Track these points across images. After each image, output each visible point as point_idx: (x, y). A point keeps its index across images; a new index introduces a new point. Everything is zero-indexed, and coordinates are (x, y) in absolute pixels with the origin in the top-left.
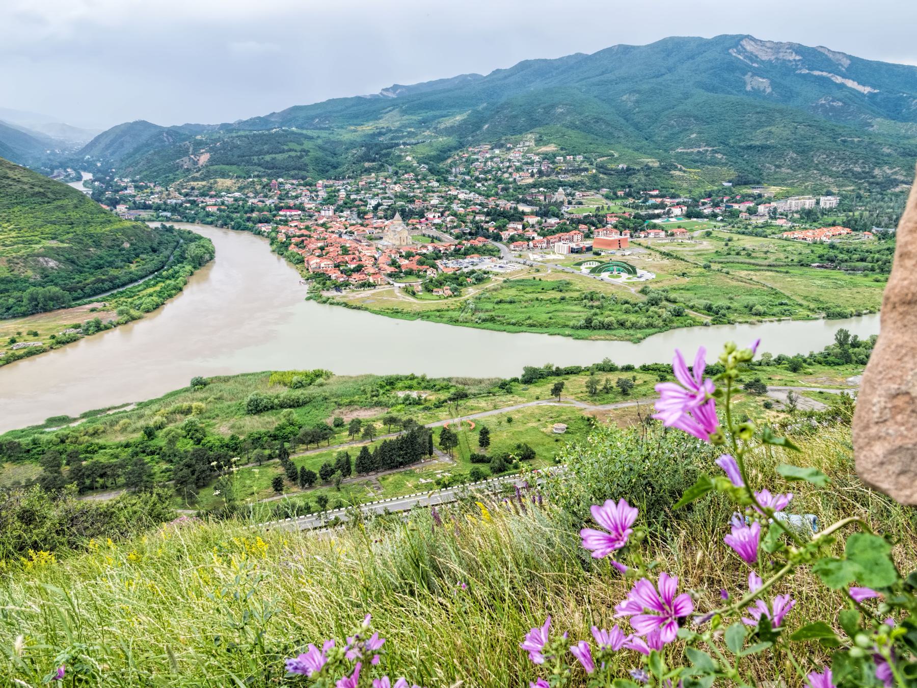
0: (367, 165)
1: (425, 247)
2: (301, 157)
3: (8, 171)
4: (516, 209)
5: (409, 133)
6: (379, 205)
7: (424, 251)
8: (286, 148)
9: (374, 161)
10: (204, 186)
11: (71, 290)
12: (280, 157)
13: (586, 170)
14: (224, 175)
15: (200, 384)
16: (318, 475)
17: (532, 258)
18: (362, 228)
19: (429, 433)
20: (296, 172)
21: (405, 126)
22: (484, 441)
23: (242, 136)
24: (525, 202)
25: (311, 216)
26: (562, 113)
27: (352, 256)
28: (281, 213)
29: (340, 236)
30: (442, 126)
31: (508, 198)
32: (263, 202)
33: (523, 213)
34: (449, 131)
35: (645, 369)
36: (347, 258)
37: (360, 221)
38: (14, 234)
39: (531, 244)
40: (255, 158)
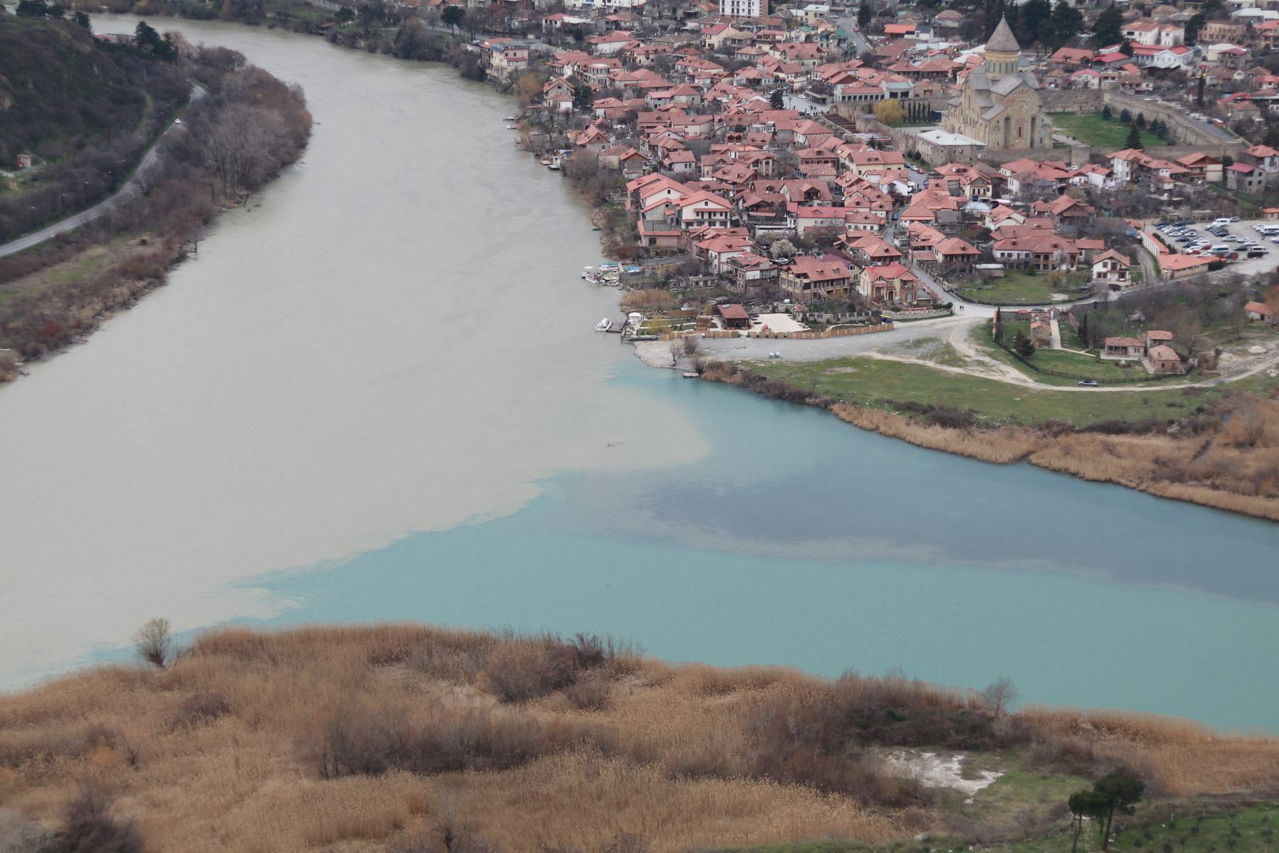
1: (1098, 160)
7: (1097, 179)
18: (865, 73)
27: (806, 187)
29: (776, 102)
37: (861, 44)
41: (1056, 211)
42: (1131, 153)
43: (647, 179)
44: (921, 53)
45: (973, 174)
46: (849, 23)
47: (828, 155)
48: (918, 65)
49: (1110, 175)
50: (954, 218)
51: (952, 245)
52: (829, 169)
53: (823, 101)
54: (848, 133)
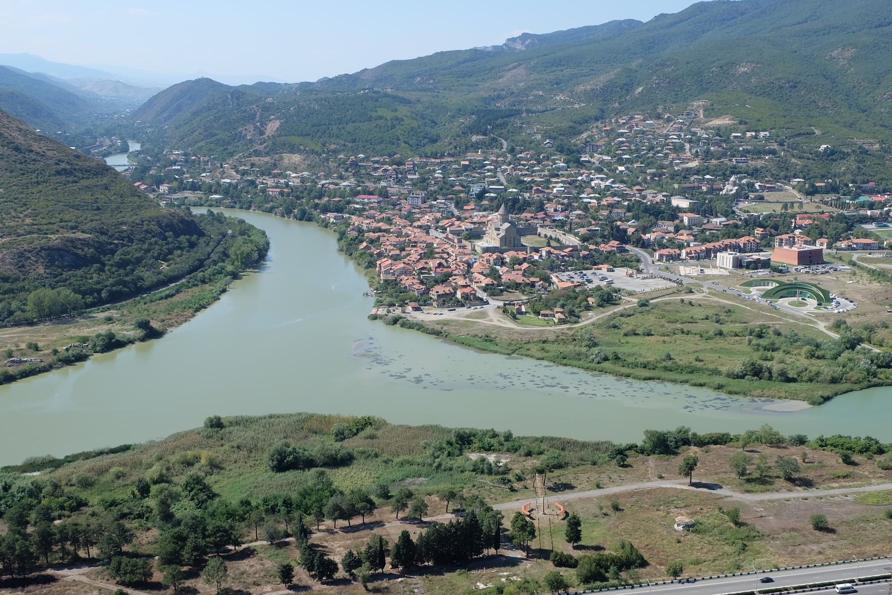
0: (474, 138)
1: (536, 250)
4: (670, 202)
5: (536, 96)
6: (484, 191)
7: (536, 257)
8: (374, 114)
9: (485, 134)
13: (773, 152)
14: (293, 150)
16: (340, 566)
17: (682, 273)
18: (457, 223)
19: (497, 518)
21: (532, 88)
22: (574, 532)
24: (682, 193)
25: (394, 205)
26: (745, 73)
27: (438, 261)
29: (428, 233)
31: (661, 187)
32: (337, 184)
33: (679, 209)
34: (590, 96)
35: (823, 444)
36: (432, 264)
37: (456, 212)
38: (28, 221)
41: (523, 269)
42: (548, 249)
43: (383, 260)
44: (476, 216)
45: (495, 256)
46: (452, 207)
48: (475, 220)
49: (541, 256)
51: (489, 281)
52: (445, 256)
53: (443, 233)
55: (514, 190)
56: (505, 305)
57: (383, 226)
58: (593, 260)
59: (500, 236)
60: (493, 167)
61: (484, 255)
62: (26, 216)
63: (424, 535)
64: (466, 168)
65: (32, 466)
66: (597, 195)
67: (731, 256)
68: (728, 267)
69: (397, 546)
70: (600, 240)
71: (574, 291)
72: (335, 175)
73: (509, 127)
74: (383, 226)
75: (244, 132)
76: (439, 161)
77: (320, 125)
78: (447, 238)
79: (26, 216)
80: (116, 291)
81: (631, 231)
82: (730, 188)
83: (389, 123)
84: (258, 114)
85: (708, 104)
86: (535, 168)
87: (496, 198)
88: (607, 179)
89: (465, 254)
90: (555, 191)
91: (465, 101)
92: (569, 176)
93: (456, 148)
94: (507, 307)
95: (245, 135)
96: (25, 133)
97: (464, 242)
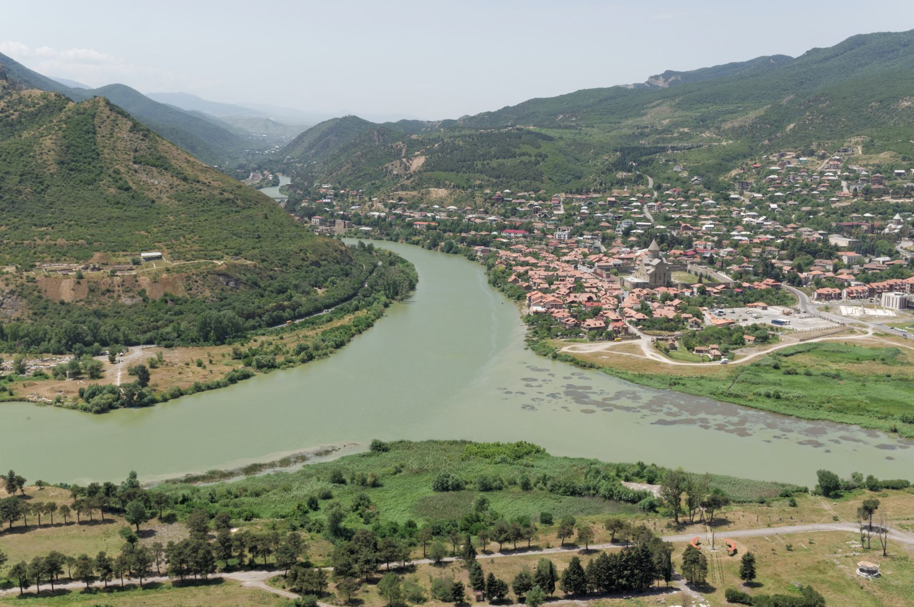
0: (621, 175)
1: (688, 286)
2: (537, 163)
3: (199, 173)
4: (827, 240)
5: (681, 134)
6: (631, 228)
8: (518, 151)
9: (629, 171)
10: (414, 197)
11: (250, 316)
12: (509, 162)
14: (438, 185)
15: (379, 448)
19: (667, 550)
20: (528, 182)
21: (676, 125)
22: (748, 570)
23: (465, 136)
24: (839, 231)
26: (909, 107)
27: (588, 295)
28: (504, 234)
29: (576, 267)
30: (727, 126)
31: (817, 225)
32: (483, 219)
33: (837, 248)
34: (737, 133)
36: (583, 297)
37: (603, 249)
39: (845, 292)
40: (479, 164)
41: (674, 304)
43: (533, 293)
45: (645, 291)
46: (598, 243)
47: (594, 285)
48: (623, 256)
49: (692, 293)
50: (639, 306)
51: (640, 316)
52: (595, 290)
53: (591, 268)
54: (600, 278)
55: (662, 227)
56: (657, 339)
57: (532, 260)
58: (745, 298)
59: (649, 272)
60: (639, 204)
61: (634, 290)
62: (193, 242)
63: (594, 562)
64: (612, 204)
65: (212, 476)
66: (748, 233)
67: (898, 297)
68: (894, 308)
69: (566, 573)
70: (753, 278)
71: (729, 329)
72: (482, 210)
73: (654, 164)
74: (532, 260)
75: (390, 167)
76: (584, 197)
77: (464, 161)
78: (595, 273)
79: (193, 242)
80: (277, 316)
81: (786, 269)
82: (893, 227)
83: (533, 159)
84: (404, 151)
85: (868, 140)
86: (683, 205)
87: (642, 234)
88: (759, 216)
89: (615, 289)
90: (704, 228)
91: (608, 138)
92: (719, 213)
93: (601, 184)
94: (661, 342)
95: (392, 170)
96: (192, 165)
97: (613, 277)
